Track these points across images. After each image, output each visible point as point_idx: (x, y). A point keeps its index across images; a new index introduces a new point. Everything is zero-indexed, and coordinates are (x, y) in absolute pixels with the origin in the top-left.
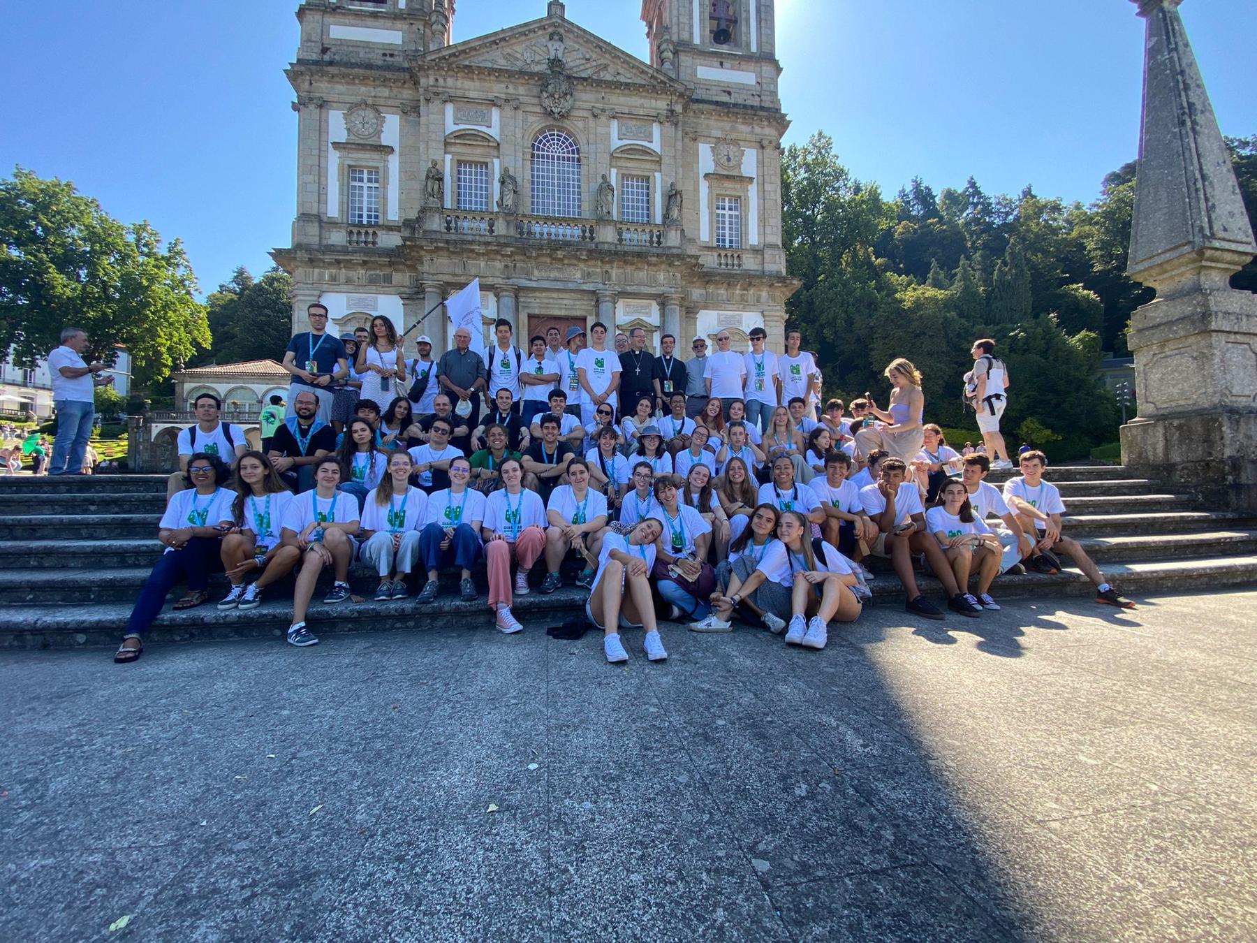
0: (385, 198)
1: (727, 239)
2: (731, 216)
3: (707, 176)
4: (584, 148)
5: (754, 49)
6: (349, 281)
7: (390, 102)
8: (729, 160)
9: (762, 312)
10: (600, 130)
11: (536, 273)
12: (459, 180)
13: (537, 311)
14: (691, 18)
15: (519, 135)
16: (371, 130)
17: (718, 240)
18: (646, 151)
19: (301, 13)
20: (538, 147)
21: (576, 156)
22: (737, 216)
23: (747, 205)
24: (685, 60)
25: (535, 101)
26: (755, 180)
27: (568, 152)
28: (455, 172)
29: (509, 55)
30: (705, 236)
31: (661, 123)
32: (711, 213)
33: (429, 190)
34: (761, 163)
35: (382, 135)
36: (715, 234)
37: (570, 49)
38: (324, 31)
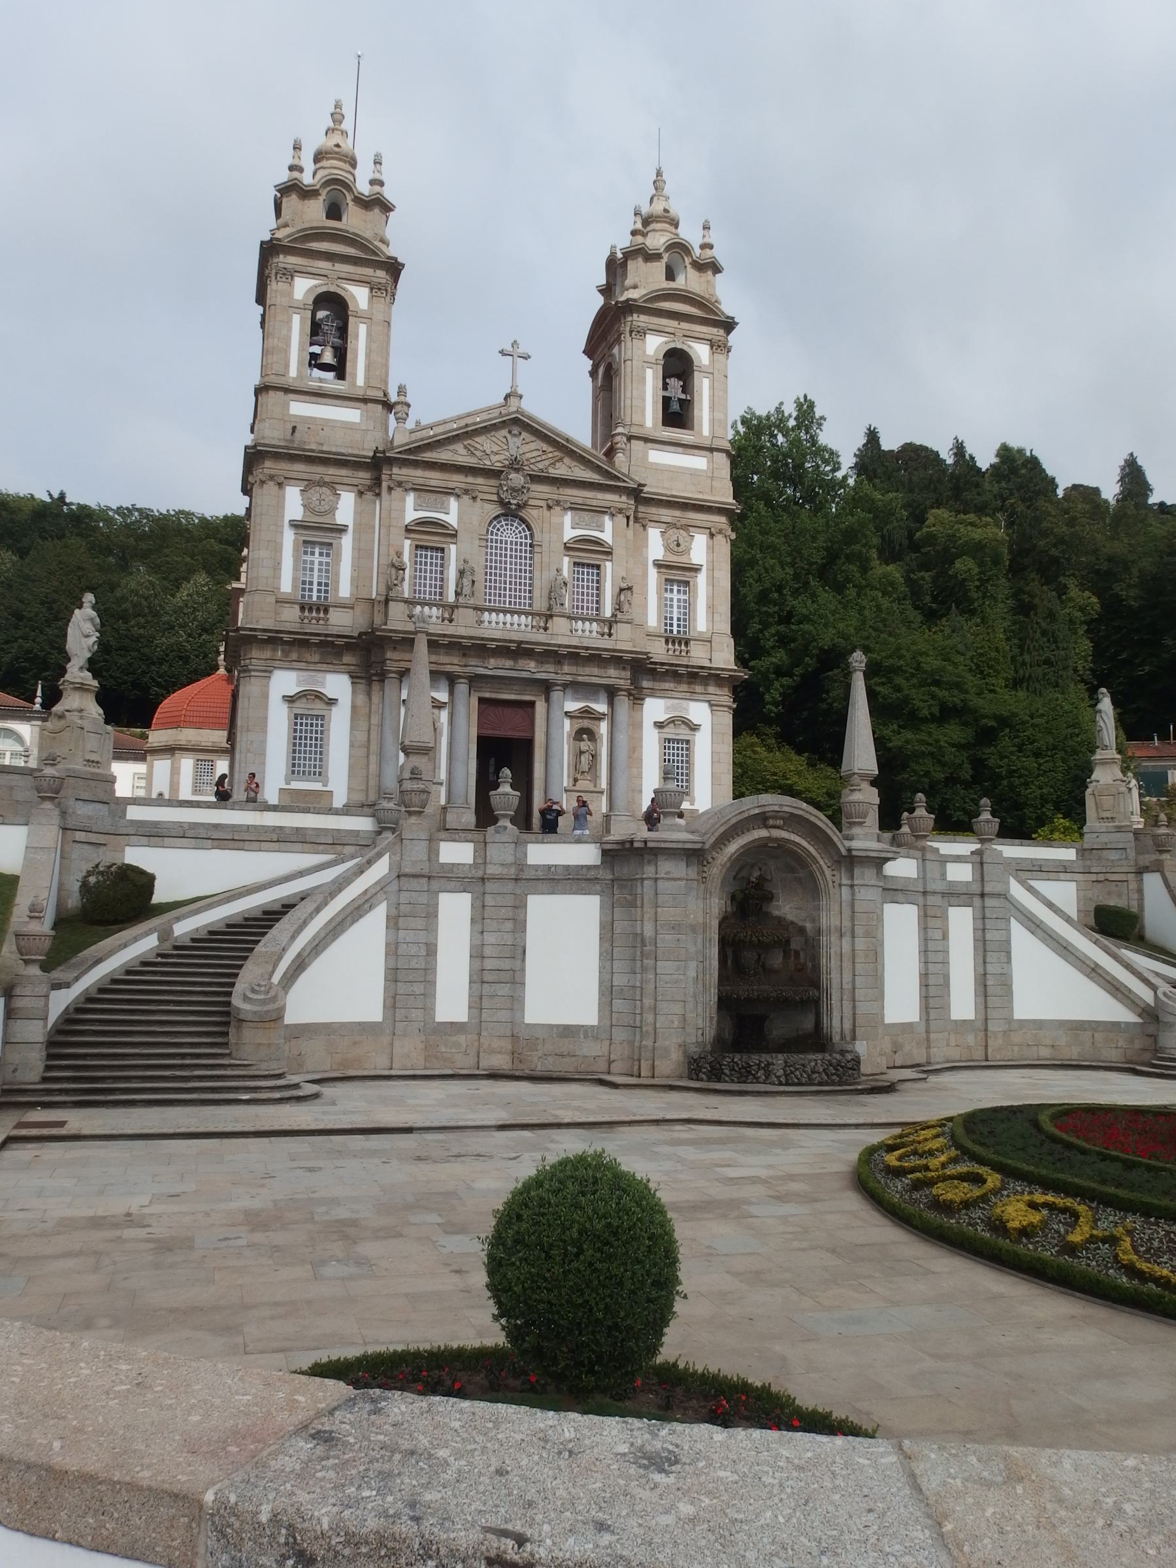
0: (337, 575)
1: (675, 622)
2: (679, 601)
4: (537, 537)
5: (706, 431)
7: (346, 480)
8: (678, 545)
9: (709, 701)
10: (555, 520)
11: (492, 661)
12: (416, 563)
13: (487, 695)
14: (644, 400)
15: (476, 523)
16: (327, 507)
18: (597, 542)
20: (492, 532)
21: (529, 541)
22: (685, 601)
23: (696, 592)
24: (637, 445)
25: (494, 490)
26: (704, 569)
27: (521, 538)
28: (413, 556)
29: (469, 445)
30: (653, 620)
31: (613, 515)
32: (660, 598)
33: (394, 577)
34: (711, 549)
35: (337, 513)
37: (527, 441)
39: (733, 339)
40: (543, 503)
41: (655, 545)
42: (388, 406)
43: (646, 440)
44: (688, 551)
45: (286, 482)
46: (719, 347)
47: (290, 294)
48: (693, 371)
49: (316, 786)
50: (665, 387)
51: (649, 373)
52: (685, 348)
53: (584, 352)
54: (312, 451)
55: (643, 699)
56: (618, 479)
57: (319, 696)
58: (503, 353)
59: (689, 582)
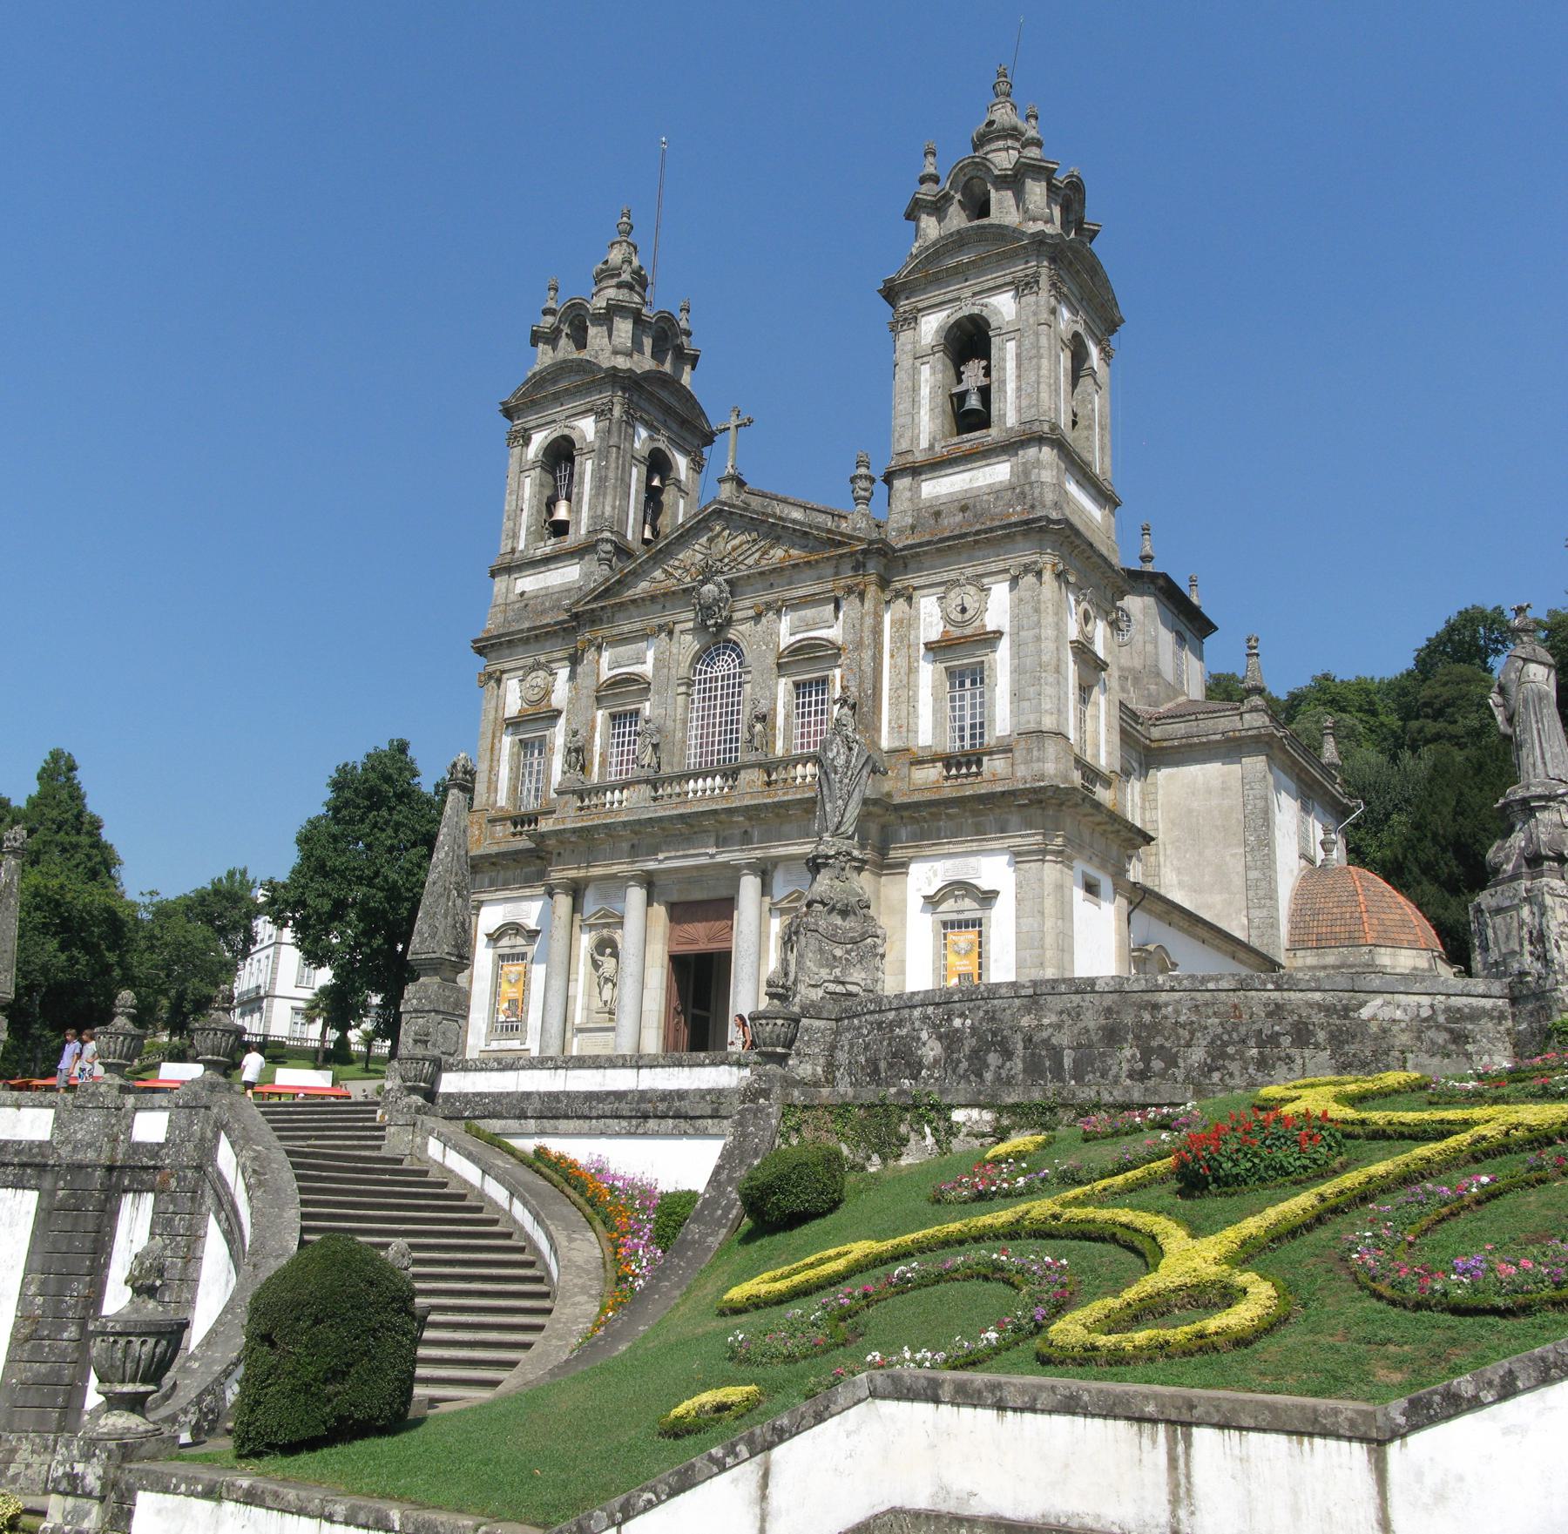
1: (967, 733)
3: (929, 647)
8: (964, 610)
35: (553, 696)
43: (916, 471)
45: (505, 676)
48: (989, 339)
49: (515, 1044)
51: (926, 371)
52: (976, 310)
54: (522, 631)
55: (904, 865)
59: (983, 662)
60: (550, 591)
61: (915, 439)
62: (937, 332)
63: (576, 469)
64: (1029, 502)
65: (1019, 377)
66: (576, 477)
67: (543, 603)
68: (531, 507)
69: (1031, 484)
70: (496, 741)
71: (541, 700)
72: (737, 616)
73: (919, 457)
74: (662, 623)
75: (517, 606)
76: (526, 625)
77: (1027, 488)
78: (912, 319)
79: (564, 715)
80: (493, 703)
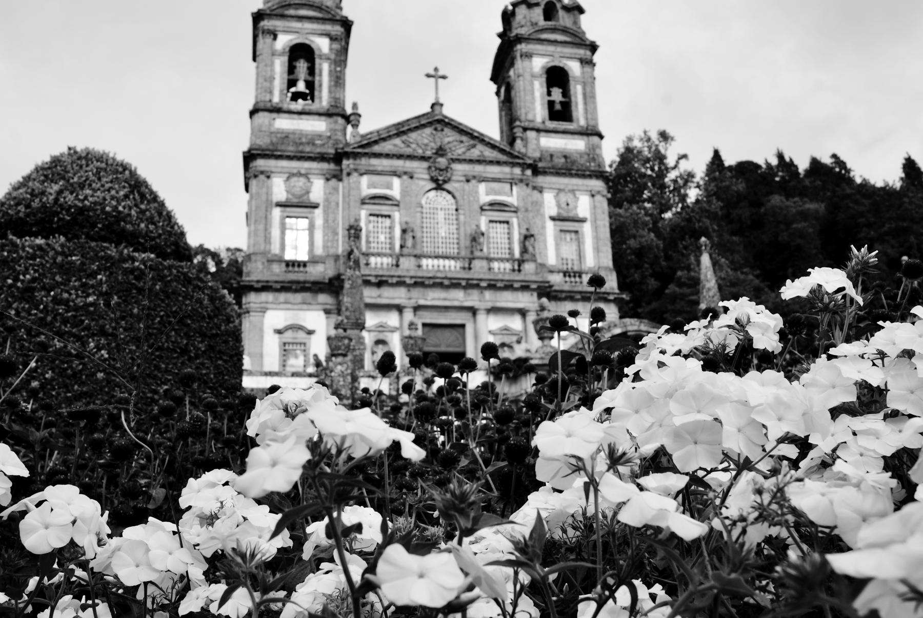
3: (553, 219)
4: (461, 202)
6: (286, 303)
8: (568, 204)
13: (428, 321)
17: (563, 264)
19: (253, 113)
25: (426, 171)
34: (594, 208)
36: (560, 259)
37: (449, 134)
38: (270, 125)
39: (596, 58)
40: (463, 179)
41: (550, 203)
42: (347, 119)
43: (538, 130)
44: (576, 207)
46: (588, 63)
47: (272, 46)
50: (549, 94)
53: (492, 79)
56: (517, 157)
57: (300, 328)
58: (428, 76)
60: (304, 133)
61: (535, 116)
62: (543, 67)
63: (317, 66)
64: (597, 164)
65: (585, 104)
66: (317, 71)
67: (300, 139)
68: (282, 78)
69: (597, 155)
70: (268, 214)
71: (301, 196)
72: (454, 178)
73: (541, 126)
74: (405, 170)
75: (279, 135)
76: (291, 148)
77: (596, 156)
78: (528, 56)
79: (321, 207)
80: (264, 190)
